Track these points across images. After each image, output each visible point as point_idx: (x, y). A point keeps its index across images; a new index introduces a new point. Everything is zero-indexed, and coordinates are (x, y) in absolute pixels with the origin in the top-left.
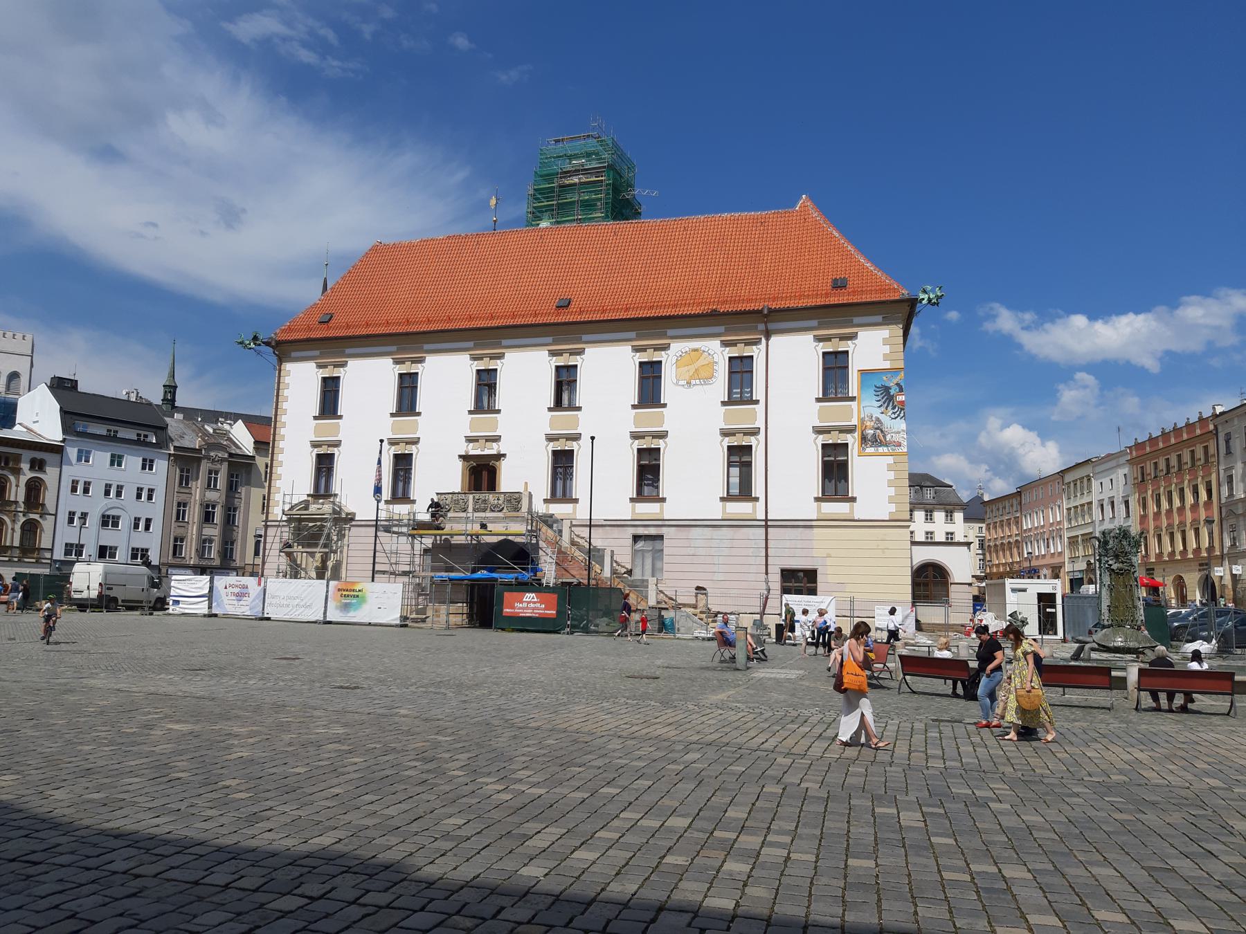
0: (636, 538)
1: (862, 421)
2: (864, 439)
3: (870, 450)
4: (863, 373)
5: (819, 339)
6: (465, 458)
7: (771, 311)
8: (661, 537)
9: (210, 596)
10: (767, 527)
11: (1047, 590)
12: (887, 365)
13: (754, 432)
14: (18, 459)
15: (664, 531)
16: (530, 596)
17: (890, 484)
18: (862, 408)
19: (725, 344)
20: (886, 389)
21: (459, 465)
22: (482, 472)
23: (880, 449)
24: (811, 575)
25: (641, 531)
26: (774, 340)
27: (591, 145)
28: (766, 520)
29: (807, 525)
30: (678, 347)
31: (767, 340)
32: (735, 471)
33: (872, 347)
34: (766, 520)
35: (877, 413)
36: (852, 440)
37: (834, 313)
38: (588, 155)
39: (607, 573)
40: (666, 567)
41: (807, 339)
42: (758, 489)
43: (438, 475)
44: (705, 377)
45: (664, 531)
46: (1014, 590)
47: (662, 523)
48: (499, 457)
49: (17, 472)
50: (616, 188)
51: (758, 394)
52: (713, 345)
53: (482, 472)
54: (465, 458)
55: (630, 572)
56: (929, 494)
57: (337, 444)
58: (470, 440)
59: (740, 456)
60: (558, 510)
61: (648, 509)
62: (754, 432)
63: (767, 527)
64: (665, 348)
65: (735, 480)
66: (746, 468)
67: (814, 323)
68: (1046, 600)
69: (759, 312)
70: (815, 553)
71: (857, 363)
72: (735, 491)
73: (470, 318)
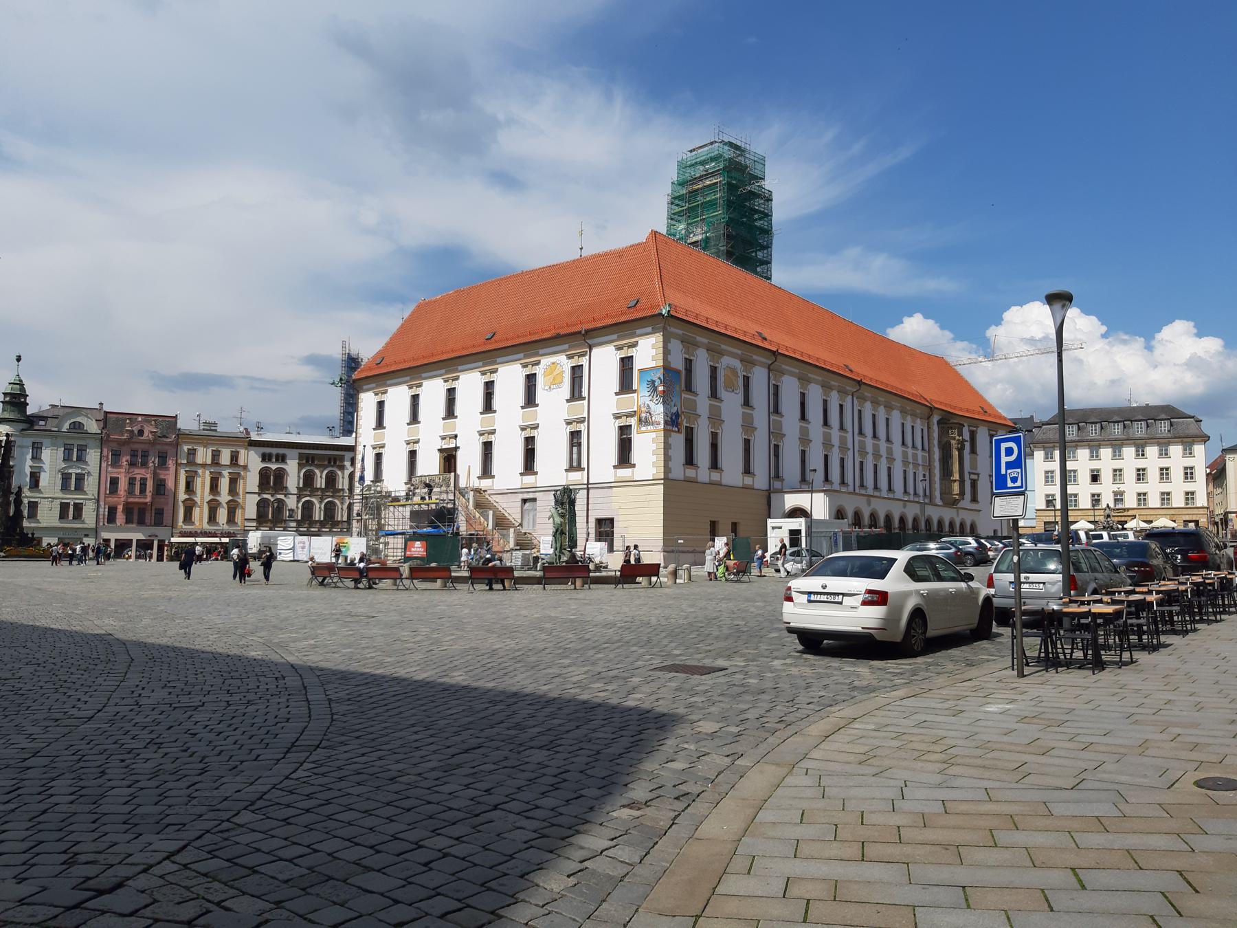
0: (525, 501)
1: (639, 407)
2: (640, 420)
3: (643, 429)
4: (641, 371)
5: (619, 348)
6: (440, 450)
7: (587, 332)
8: (534, 500)
9: (293, 549)
10: (588, 489)
11: (795, 527)
12: (653, 364)
13: (581, 421)
14: (342, 459)
15: (537, 495)
16: (418, 544)
17: (654, 453)
18: (644, 399)
19: (570, 357)
20: (653, 382)
21: (438, 454)
22: (449, 459)
23: (650, 428)
24: (600, 522)
25: (526, 496)
26: (594, 351)
27: (716, 149)
28: (588, 484)
29: (607, 486)
30: (546, 361)
31: (591, 350)
32: (575, 449)
33: (648, 351)
34: (588, 484)
35: (647, 400)
36: (633, 421)
37: (623, 329)
38: (712, 159)
39: (490, 527)
40: (538, 521)
41: (610, 349)
42: (584, 465)
43: (429, 465)
44: (556, 382)
45: (537, 495)
46: (773, 528)
47: (535, 489)
48: (456, 448)
49: (342, 468)
50: (731, 188)
51: (585, 394)
52: (562, 358)
53: (449, 459)
54: (440, 450)
55: (521, 525)
56: (1163, 428)
57: (383, 446)
58: (443, 438)
59: (575, 437)
60: (485, 484)
61: (529, 479)
62: (581, 421)
63: (588, 489)
64: (538, 363)
65: (575, 456)
66: (579, 445)
67: (615, 337)
68: (795, 534)
69: (580, 332)
70: (614, 506)
71: (638, 365)
72: (575, 464)
73: (424, 357)
